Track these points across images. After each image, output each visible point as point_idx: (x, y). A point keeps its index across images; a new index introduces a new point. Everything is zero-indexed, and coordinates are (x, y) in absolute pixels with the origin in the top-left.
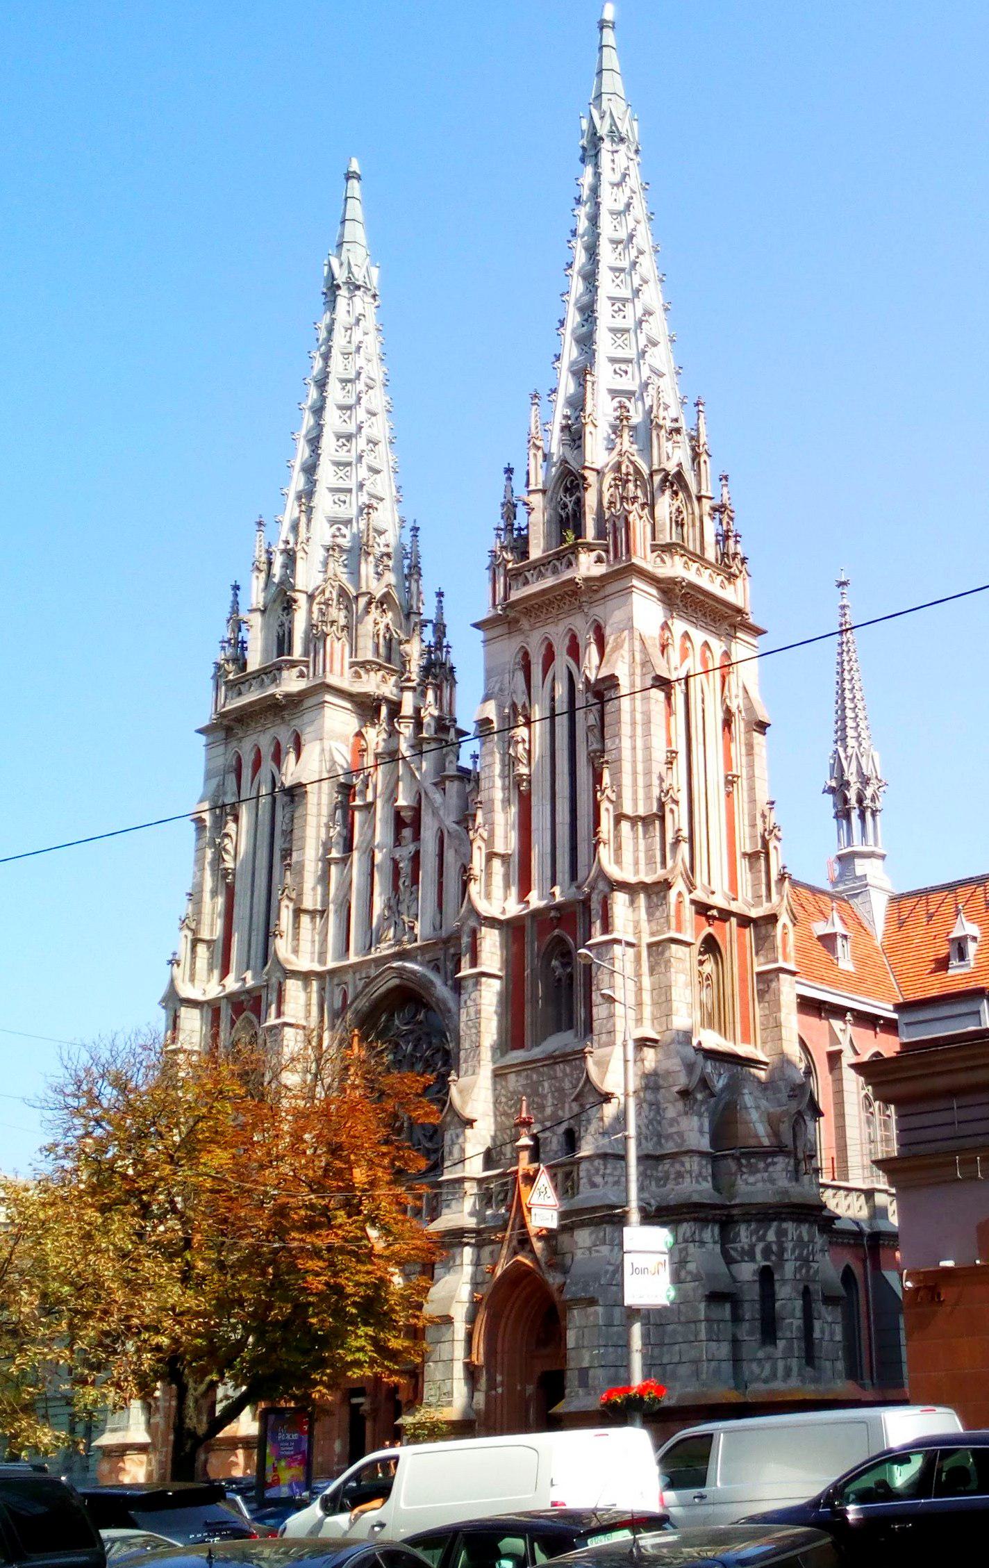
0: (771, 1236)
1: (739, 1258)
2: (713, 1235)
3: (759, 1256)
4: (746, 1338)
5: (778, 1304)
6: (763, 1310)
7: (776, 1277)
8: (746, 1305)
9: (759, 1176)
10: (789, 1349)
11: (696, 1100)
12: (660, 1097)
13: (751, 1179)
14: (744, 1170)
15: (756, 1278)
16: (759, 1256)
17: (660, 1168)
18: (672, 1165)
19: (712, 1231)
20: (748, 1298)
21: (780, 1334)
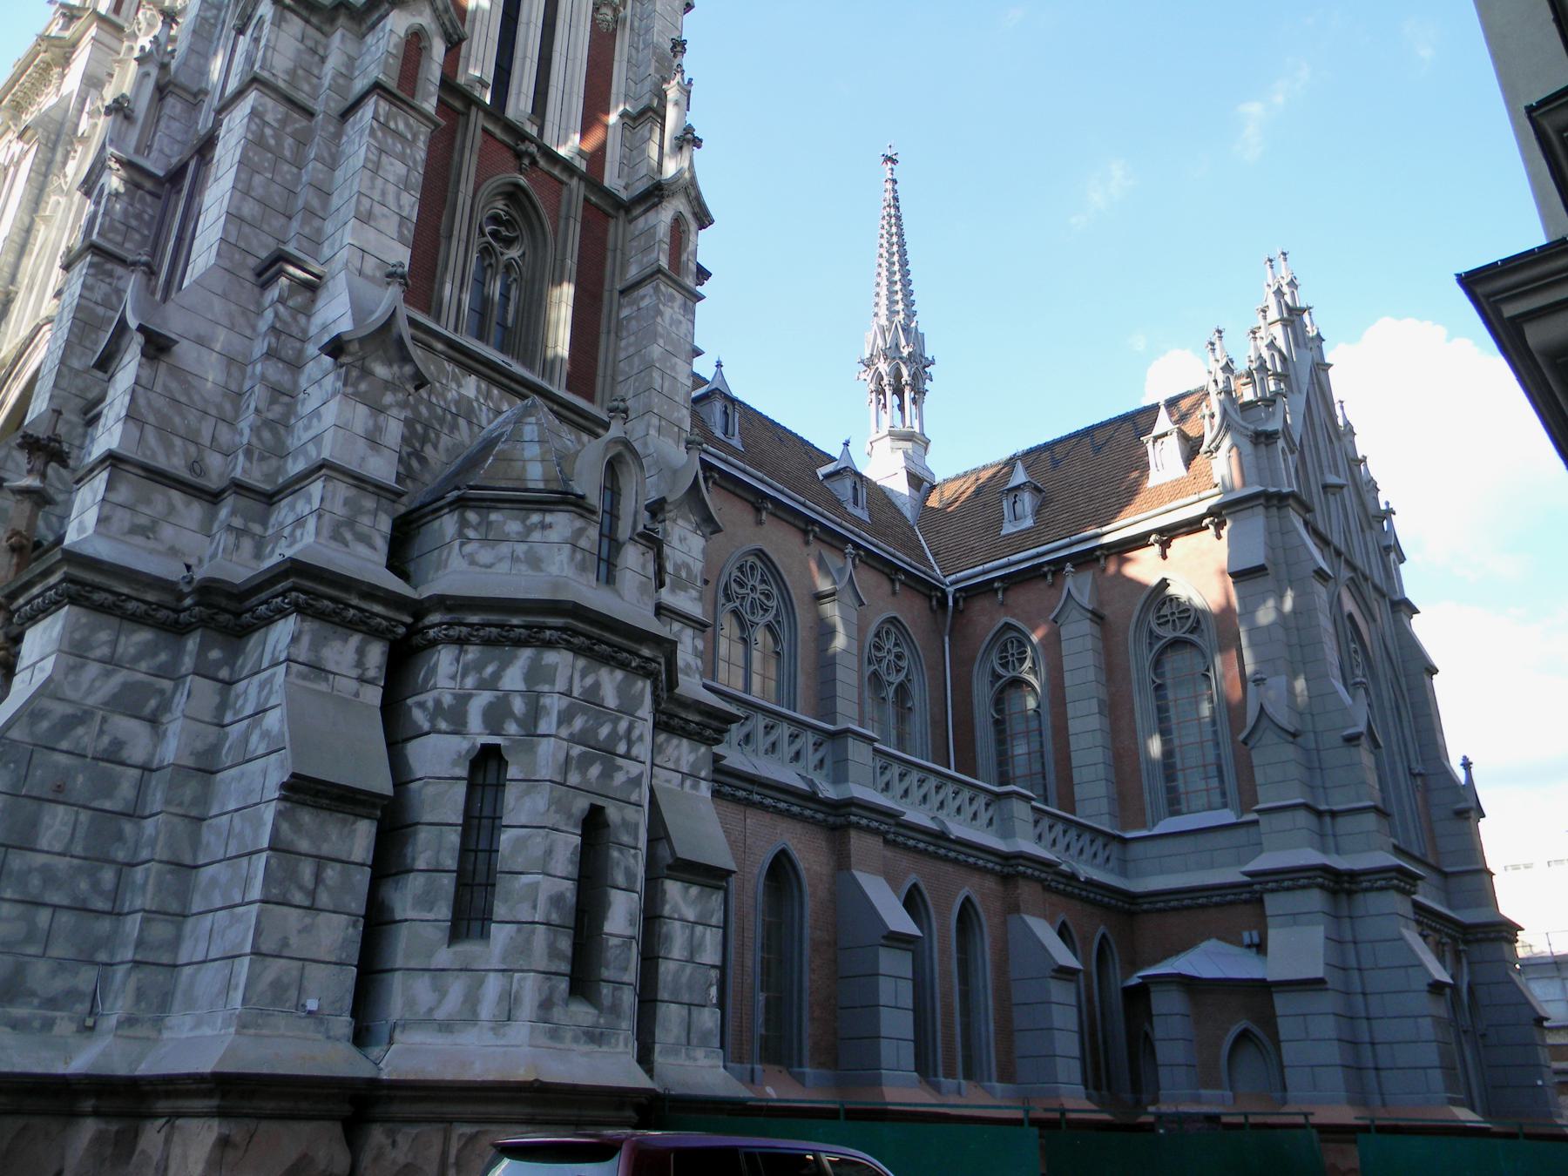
0: (513, 679)
1: (426, 726)
2: (360, 664)
3: (475, 722)
4: (410, 914)
5: (506, 837)
6: (464, 850)
7: (513, 772)
8: (424, 835)
9: (504, 548)
10: (522, 948)
11: (366, 373)
12: (303, 382)
13: (485, 556)
14: (471, 533)
15: (462, 772)
16: (475, 722)
17: (273, 520)
18: (292, 507)
19: (361, 652)
20: (427, 818)
21: (500, 910)
